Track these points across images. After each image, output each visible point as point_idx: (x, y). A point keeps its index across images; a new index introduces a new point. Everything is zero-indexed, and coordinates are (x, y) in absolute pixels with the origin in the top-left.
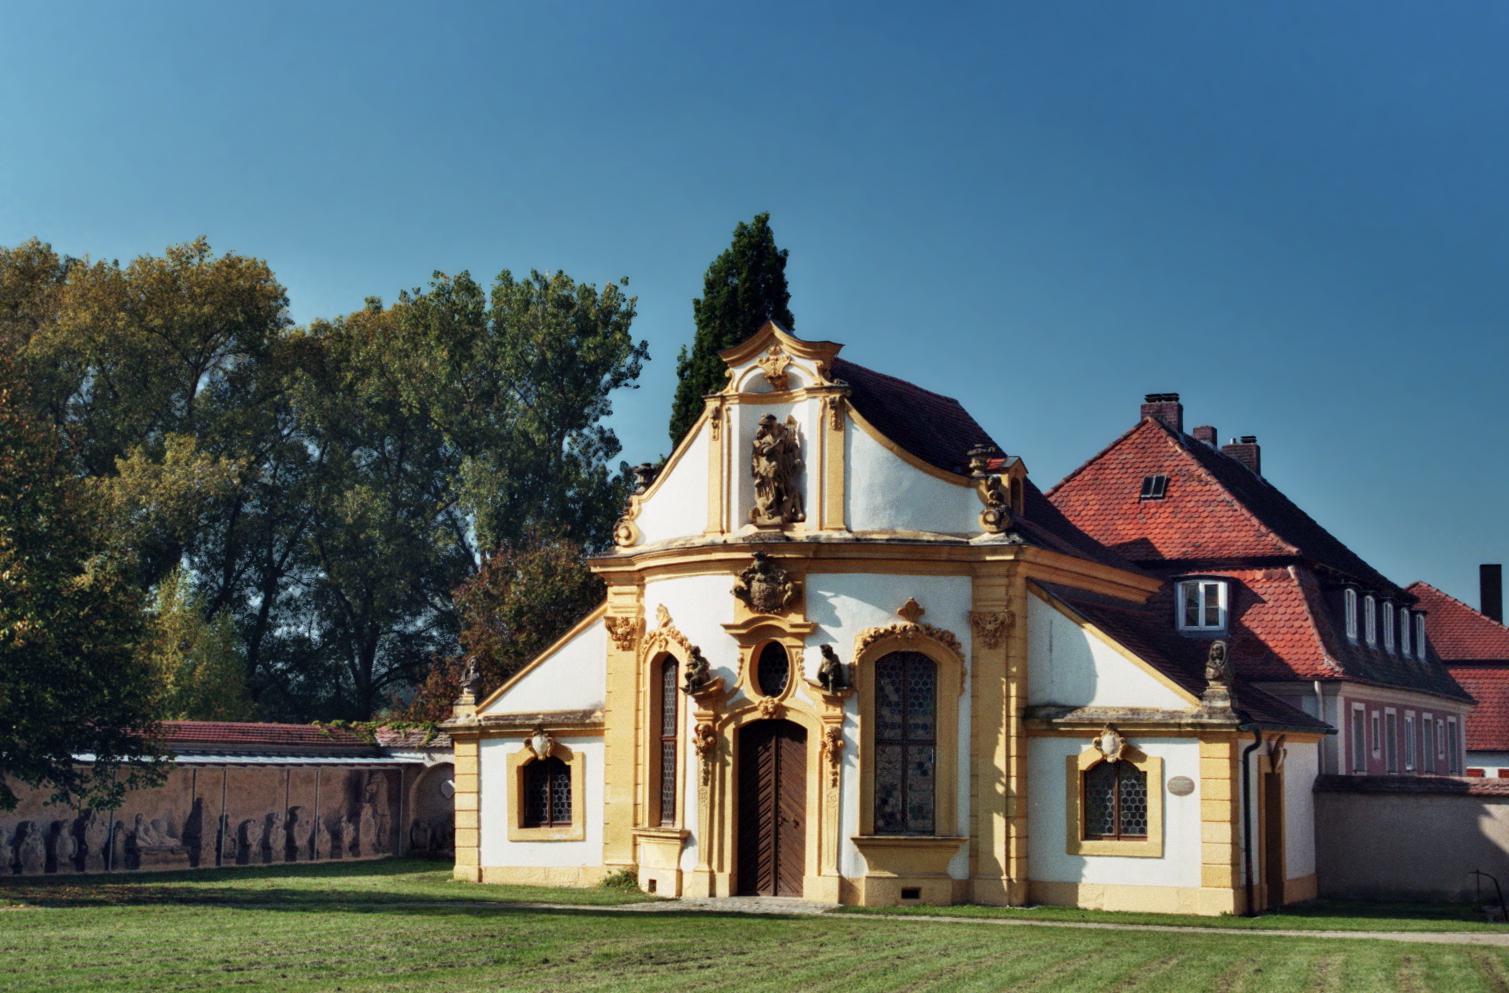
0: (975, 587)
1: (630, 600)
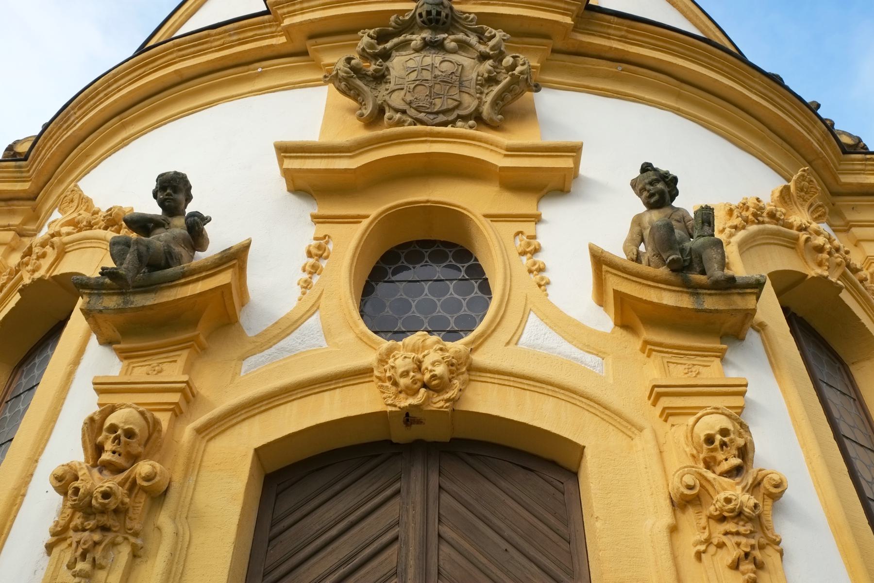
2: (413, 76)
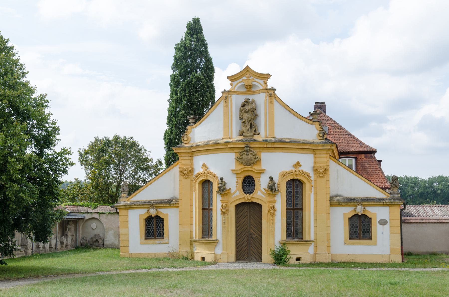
0: (315, 158)
1: (188, 162)
2: (245, 159)
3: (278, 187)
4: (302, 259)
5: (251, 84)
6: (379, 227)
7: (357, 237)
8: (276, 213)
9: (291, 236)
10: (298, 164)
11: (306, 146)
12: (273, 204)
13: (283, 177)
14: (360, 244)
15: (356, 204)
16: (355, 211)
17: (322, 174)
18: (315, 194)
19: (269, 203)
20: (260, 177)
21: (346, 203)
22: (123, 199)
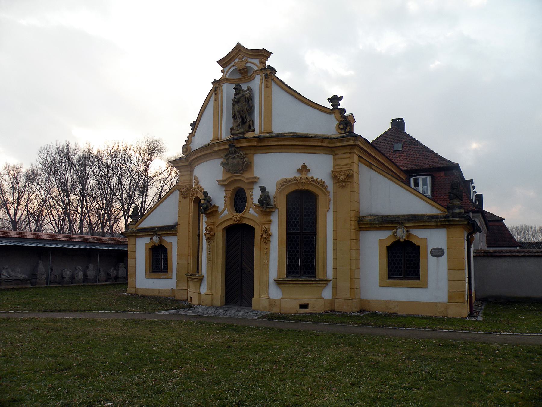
0: (335, 160)
3: (275, 201)
4: (310, 306)
5: (244, 67)
6: (432, 260)
7: (400, 275)
8: (271, 239)
9: (297, 273)
10: (304, 169)
11: (318, 142)
12: (266, 226)
13: (282, 186)
14: (402, 286)
15: (396, 225)
16: (395, 235)
17: (344, 182)
18: (335, 212)
19: (263, 224)
20: (253, 189)
21: (381, 224)
22: (132, 225)
